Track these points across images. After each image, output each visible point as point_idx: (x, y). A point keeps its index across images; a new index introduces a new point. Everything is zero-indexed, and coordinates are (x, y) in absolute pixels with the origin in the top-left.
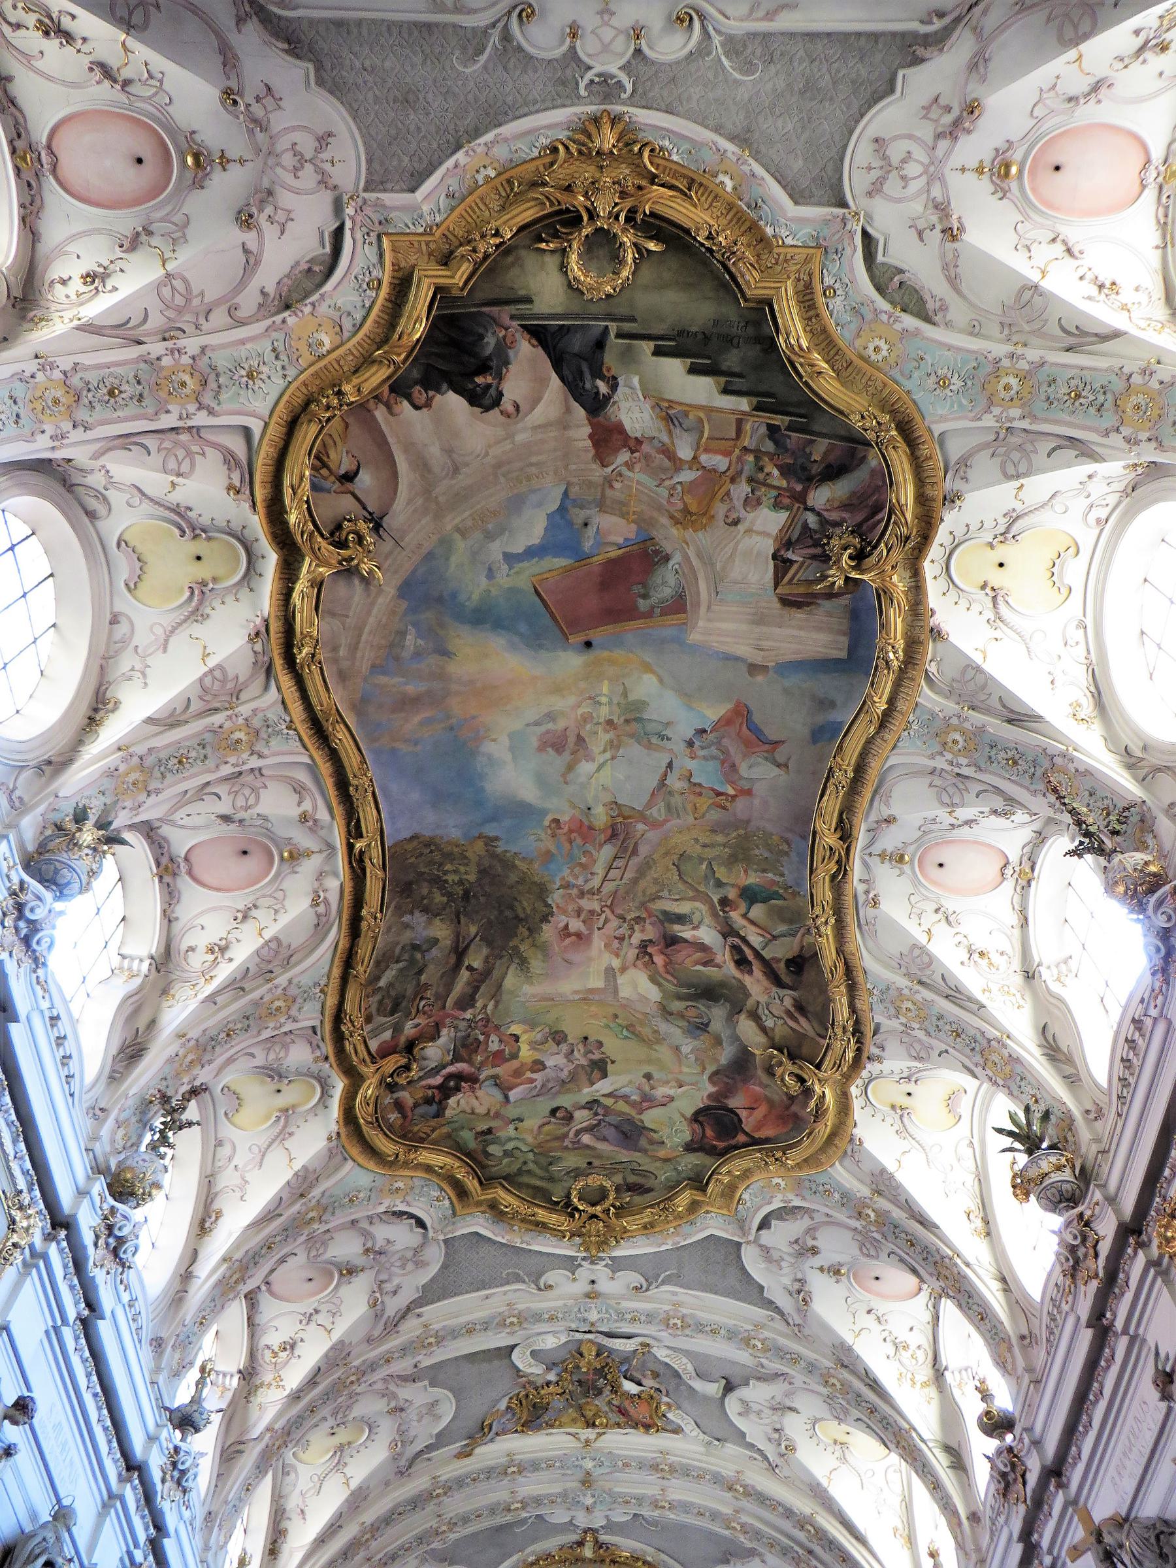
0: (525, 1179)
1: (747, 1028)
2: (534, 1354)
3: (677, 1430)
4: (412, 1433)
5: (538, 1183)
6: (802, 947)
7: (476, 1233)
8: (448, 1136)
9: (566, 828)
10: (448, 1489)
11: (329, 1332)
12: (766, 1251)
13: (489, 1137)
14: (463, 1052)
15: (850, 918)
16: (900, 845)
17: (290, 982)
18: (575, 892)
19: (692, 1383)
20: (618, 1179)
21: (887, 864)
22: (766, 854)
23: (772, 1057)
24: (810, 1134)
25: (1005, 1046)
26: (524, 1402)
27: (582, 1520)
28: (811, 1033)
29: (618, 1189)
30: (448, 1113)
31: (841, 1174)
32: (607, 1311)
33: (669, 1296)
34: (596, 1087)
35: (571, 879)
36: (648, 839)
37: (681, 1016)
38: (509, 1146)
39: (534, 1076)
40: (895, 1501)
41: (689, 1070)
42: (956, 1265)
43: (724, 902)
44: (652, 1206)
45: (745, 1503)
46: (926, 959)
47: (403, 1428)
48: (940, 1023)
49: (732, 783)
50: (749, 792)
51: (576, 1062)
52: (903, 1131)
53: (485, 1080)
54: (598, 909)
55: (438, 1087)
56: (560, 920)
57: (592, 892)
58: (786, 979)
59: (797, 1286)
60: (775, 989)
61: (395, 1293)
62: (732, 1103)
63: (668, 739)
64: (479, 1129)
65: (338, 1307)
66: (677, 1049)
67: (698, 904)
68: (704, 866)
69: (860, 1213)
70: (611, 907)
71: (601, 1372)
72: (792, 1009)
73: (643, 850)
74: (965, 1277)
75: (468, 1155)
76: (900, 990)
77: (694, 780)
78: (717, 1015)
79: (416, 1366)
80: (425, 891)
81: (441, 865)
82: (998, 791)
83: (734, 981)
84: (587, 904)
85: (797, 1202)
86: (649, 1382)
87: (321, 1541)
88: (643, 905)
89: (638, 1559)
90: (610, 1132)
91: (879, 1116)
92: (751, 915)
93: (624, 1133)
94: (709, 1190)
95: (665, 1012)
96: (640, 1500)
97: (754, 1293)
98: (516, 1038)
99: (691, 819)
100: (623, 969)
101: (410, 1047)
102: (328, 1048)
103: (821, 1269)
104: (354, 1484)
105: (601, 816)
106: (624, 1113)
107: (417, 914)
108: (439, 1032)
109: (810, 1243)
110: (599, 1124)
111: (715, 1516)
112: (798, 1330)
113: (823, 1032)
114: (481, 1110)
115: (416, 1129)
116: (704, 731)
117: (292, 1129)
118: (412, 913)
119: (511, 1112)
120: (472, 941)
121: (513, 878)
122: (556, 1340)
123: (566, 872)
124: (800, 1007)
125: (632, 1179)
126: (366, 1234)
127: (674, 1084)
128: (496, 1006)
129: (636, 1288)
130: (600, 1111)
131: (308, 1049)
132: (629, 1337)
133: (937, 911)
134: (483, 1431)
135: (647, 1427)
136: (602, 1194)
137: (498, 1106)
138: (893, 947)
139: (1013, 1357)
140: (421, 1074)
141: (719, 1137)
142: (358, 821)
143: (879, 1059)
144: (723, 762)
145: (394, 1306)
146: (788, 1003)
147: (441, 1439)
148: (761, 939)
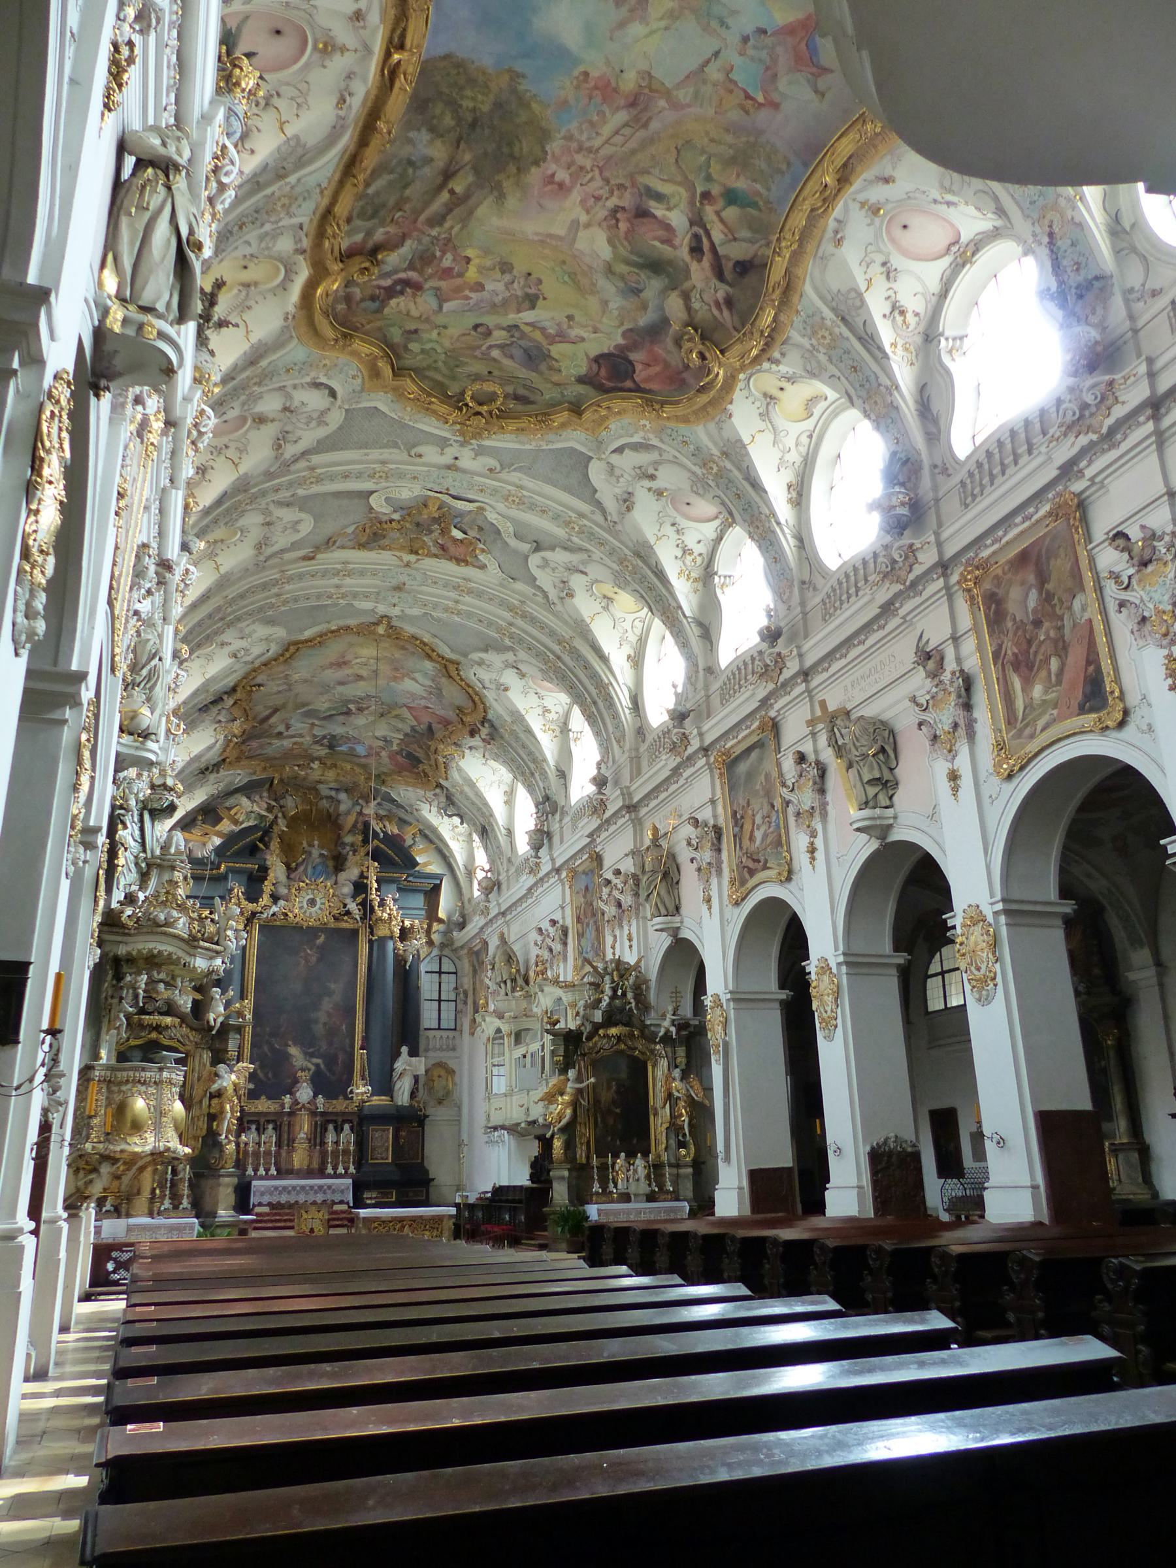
0: (431, 374)
1: (674, 306)
2: (387, 500)
3: (483, 567)
4: (274, 539)
5: (439, 378)
6: (755, 255)
8: (380, 329)
9: (592, 84)
10: (290, 580)
11: (236, 465)
12: (611, 468)
14: (418, 264)
15: (810, 247)
16: (882, 200)
17: (299, 180)
18: (574, 145)
19: (508, 540)
20: (510, 389)
21: (863, 212)
22: (763, 165)
23: (688, 333)
24: (689, 399)
25: (891, 395)
26: (368, 531)
27: (382, 609)
28: (730, 326)
29: (506, 396)
30: (386, 311)
31: (702, 434)
33: (517, 481)
35: (576, 133)
36: (663, 117)
37: (622, 277)
38: (428, 346)
39: (472, 295)
40: (633, 639)
41: (608, 322)
42: (769, 522)
43: (706, 195)
44: (530, 416)
45: (519, 622)
46: (858, 303)
48: (845, 357)
49: (765, 92)
50: (776, 106)
52: (765, 415)
54: (589, 168)
55: (385, 288)
56: (551, 168)
57: (590, 150)
58: (728, 274)
59: (626, 496)
60: (714, 281)
61: (296, 442)
62: (633, 356)
63: (728, 28)
64: (408, 328)
65: (245, 446)
66: (605, 303)
67: (682, 190)
68: (703, 158)
69: (705, 464)
70: (601, 170)
71: (436, 520)
72: (721, 301)
73: (654, 125)
74: (774, 532)
76: (823, 319)
77: (733, 76)
78: (653, 286)
80: (438, 111)
81: (462, 88)
82: (996, 199)
83: (681, 263)
84: (581, 160)
85: (655, 441)
86: (473, 533)
87: (194, 606)
88: (631, 176)
89: (417, 639)
90: (518, 353)
91: (751, 399)
92: (723, 214)
93: (530, 357)
94: (587, 415)
95: (609, 270)
96: (435, 606)
97: (589, 492)
98: (468, 260)
99: (711, 112)
100: (588, 225)
101: (374, 251)
102: (306, 243)
103: (650, 489)
104: (223, 570)
105: (629, 83)
106: (536, 341)
107: (424, 131)
109: (651, 471)
111: (490, 624)
112: (612, 528)
113: (738, 326)
116: (765, 32)
117: (251, 303)
118: (419, 130)
119: (440, 320)
120: (461, 168)
121: (523, 117)
123: (573, 126)
124: (729, 302)
125: (521, 391)
126: (289, 397)
127: (590, 329)
128: (462, 229)
129: (491, 470)
130: (517, 334)
132: (470, 501)
133: (884, 264)
134: (329, 543)
135: (459, 561)
136: (491, 398)
138: (835, 283)
139: (791, 592)
141: (608, 379)
142: (405, 30)
143: (777, 362)
144: (768, 69)
145: (290, 451)
146: (720, 295)
147: (294, 546)
148: (722, 236)
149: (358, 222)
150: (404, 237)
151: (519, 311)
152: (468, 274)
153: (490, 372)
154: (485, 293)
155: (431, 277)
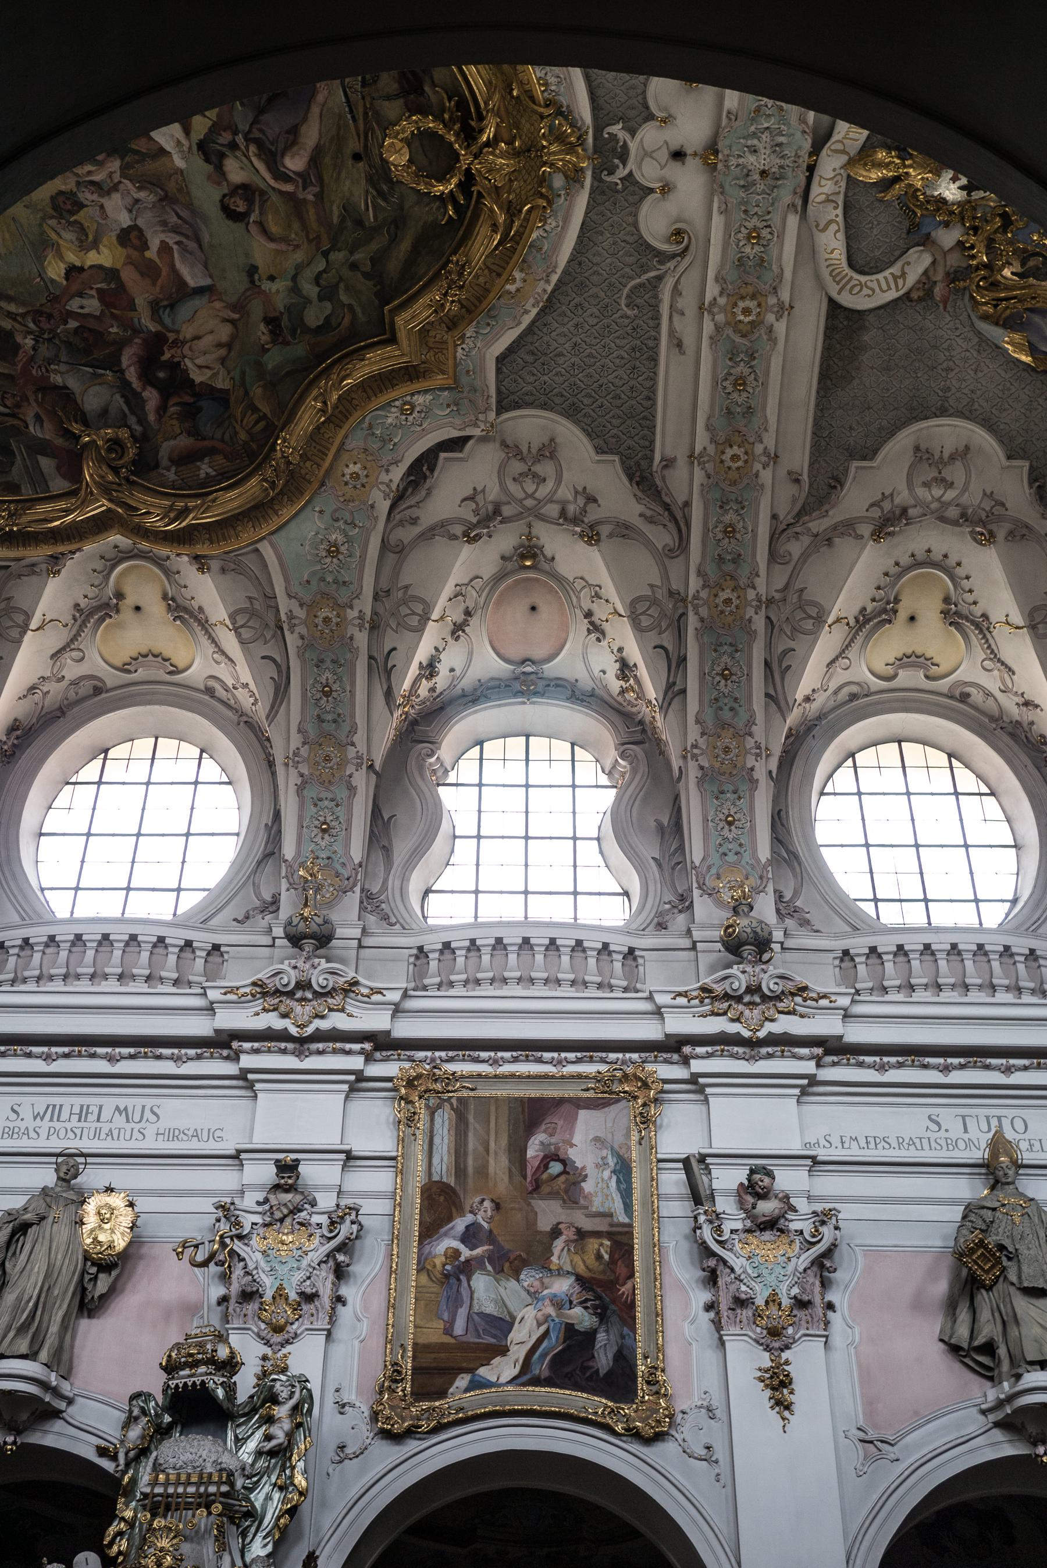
4: (973, 498)
5: (405, 246)
7: (500, 360)
13: (285, 321)
20: (391, 109)
32: (754, 135)
34: (168, 148)
38: (311, 290)
39: (154, 244)
47: (953, 513)
51: (117, 178)
53: (161, 322)
61: (592, 499)
64: (265, 338)
75: (321, 358)
79: (797, 481)
90: (274, 125)
98: (73, 271)
102: (38, 553)
104: (1017, 619)
108: (56, 387)
110: (259, 144)
114: (224, 332)
115: (243, 436)
119: (234, 283)
122: (833, 227)
130: (226, 138)
131: (34, 579)
137: (218, 305)
140: (132, 420)
149: (16, 472)
150: (46, 388)
151: (162, 152)
152: (107, 263)
153: (357, 157)
154: (140, 222)
155: (127, 325)
